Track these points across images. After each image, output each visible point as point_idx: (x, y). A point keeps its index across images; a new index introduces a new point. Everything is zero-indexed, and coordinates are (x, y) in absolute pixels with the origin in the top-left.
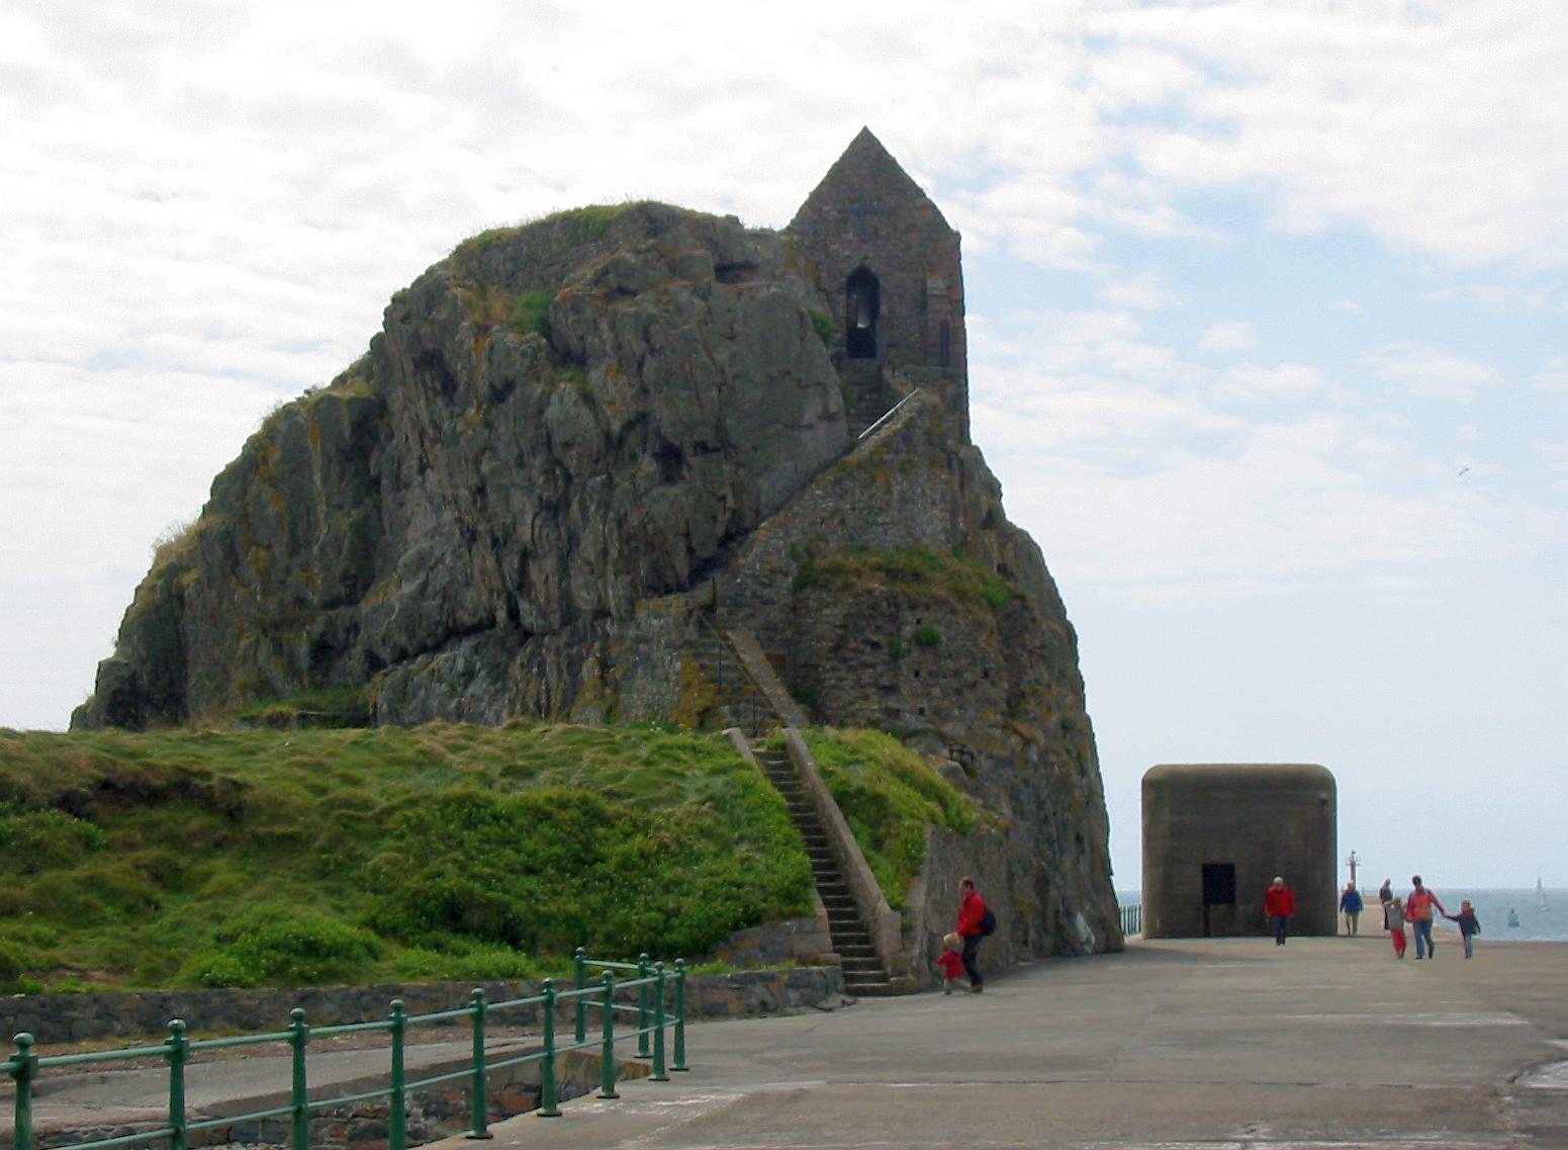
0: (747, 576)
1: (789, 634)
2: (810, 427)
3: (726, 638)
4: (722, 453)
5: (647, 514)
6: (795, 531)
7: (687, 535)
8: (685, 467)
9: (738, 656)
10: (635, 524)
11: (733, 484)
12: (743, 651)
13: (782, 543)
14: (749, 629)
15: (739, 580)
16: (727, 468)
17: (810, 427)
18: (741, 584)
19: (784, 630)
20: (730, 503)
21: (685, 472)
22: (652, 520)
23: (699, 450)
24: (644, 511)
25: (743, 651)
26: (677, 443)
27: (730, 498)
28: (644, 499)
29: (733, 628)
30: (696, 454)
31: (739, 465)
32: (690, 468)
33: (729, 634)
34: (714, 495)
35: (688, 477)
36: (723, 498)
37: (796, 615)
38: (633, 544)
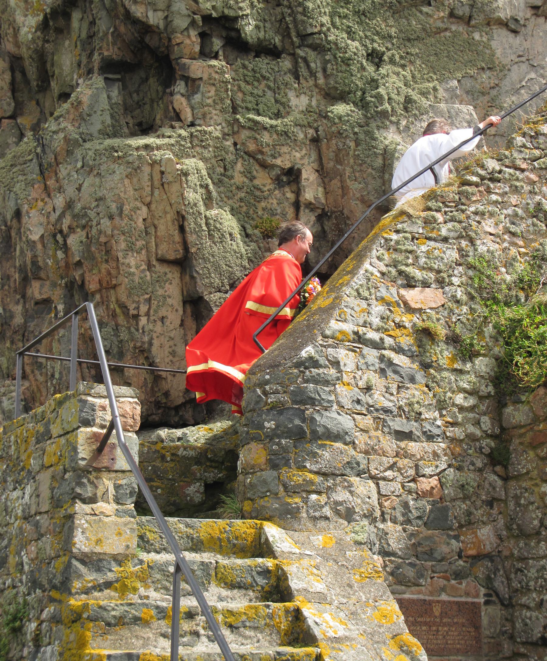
0: (338, 340)
1: (486, 534)
2: (512, 26)
3: (262, 548)
4: (286, 63)
5: (69, 205)
6: (488, 226)
7: (184, 263)
8: (180, 87)
9: (297, 615)
10: (35, 237)
11: (315, 140)
12: (321, 599)
13: (453, 255)
14: (349, 515)
15: (308, 351)
16: (299, 102)
17: (512, 26)
18: (313, 363)
19: (469, 523)
20: (312, 191)
21: (180, 102)
22: (82, 221)
23: (217, 44)
24: (59, 201)
25: (321, 599)
26: (154, 18)
27: (309, 175)
28: (63, 171)
29: (286, 517)
30: (206, 53)
31: (334, 96)
32: (193, 84)
33: (273, 531)
34: (264, 165)
35: (188, 115)
36: (292, 176)
37: (506, 479)
38: (36, 290)
